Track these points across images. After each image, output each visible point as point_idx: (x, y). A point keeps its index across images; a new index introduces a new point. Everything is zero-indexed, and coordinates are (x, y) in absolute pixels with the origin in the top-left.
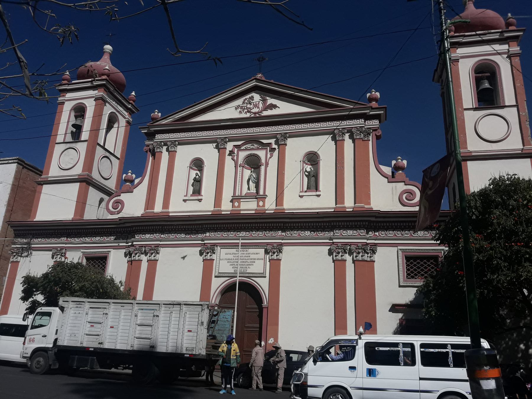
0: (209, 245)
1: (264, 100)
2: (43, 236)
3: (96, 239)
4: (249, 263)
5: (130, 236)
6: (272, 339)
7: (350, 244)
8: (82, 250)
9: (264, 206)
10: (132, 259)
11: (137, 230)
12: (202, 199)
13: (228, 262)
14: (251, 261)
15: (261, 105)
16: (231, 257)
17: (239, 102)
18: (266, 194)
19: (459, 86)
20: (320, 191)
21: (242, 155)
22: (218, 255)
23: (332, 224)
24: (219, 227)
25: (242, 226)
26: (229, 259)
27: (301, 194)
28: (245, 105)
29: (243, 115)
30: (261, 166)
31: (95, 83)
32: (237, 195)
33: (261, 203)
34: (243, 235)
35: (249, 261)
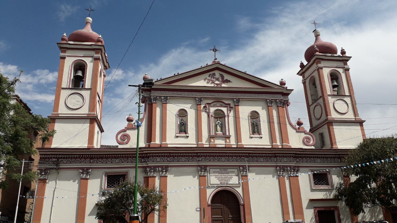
1: (222, 77)
7: (287, 167)
8: (104, 170)
9: (230, 142)
12: (188, 136)
13: (216, 177)
15: (220, 80)
17: (206, 75)
18: (230, 135)
19: (324, 82)
20: (262, 135)
21: (212, 110)
23: (276, 155)
26: (216, 176)
27: (252, 136)
29: (209, 85)
31: (94, 47)
33: (228, 141)
34: (223, 161)
35: (229, 177)
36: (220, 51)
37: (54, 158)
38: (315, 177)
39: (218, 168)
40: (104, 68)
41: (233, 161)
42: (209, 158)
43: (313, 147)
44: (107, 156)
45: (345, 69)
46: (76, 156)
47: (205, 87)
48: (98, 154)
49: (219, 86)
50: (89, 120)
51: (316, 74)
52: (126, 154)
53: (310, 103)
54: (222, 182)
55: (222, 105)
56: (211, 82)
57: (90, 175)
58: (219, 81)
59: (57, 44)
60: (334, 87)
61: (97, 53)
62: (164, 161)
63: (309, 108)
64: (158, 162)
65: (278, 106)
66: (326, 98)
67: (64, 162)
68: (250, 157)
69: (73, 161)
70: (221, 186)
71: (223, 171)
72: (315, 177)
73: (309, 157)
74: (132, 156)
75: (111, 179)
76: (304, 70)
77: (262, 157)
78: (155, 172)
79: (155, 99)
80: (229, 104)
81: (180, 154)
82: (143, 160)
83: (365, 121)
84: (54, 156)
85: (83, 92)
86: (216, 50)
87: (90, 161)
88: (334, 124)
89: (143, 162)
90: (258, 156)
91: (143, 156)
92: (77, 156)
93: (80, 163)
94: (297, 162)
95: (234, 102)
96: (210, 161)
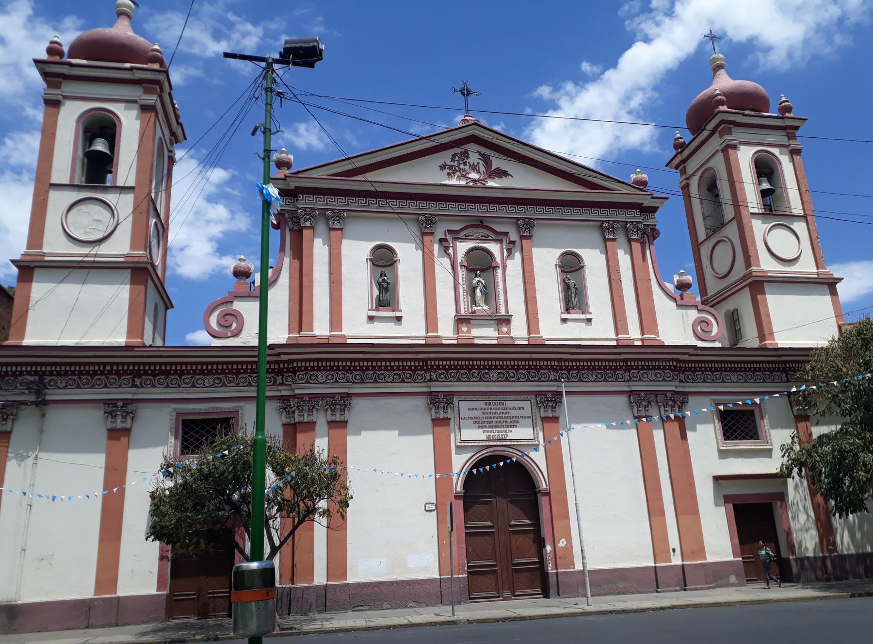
0: (441, 396)
2: (70, 377)
3: (204, 385)
4: (511, 424)
5: (280, 377)
6: (563, 540)
9: (509, 332)
10: (297, 421)
11: (302, 366)
13: (475, 423)
14: (512, 420)
15: (482, 169)
16: (478, 414)
17: (446, 157)
18: (510, 313)
20: (591, 313)
21: (463, 247)
22: (456, 412)
23: (629, 364)
24: (446, 365)
25: (475, 363)
26: (475, 418)
28: (456, 164)
29: (454, 181)
30: (495, 268)
32: (463, 312)
34: (494, 379)
35: (509, 420)
36: (478, 94)
37: (29, 373)
38: (725, 419)
39: (481, 397)
40: (171, 140)
41: (518, 380)
42: (457, 372)
43: (718, 345)
44: (179, 367)
45: (790, 148)
46: (92, 368)
47: (445, 188)
48: (155, 364)
49: (479, 185)
50: (127, 274)
51: (718, 163)
52: (232, 363)
53: (702, 235)
54: (492, 434)
55: (488, 236)
56: (458, 173)
57: (133, 419)
58: (478, 172)
59: (36, 62)
60: (764, 194)
61: (147, 91)
62: (336, 382)
63: (699, 249)
64: (320, 383)
65: (630, 241)
66: (745, 220)
67: (59, 385)
68: (563, 370)
69: (85, 381)
70: (487, 444)
71: (493, 407)
72: (725, 419)
73: (711, 370)
74: (249, 367)
75: (192, 429)
76: (686, 153)
77: (592, 370)
78: (314, 411)
79: (310, 215)
80: (506, 234)
81: (379, 364)
82: (279, 381)
83: (841, 279)
84: (29, 369)
85: (111, 198)
86: (469, 93)
87: (133, 381)
88: (765, 283)
89: (280, 384)
90: (583, 368)
91: (279, 368)
92: (97, 368)
93: (106, 387)
94: (681, 381)
95: (519, 227)
96: (459, 380)
